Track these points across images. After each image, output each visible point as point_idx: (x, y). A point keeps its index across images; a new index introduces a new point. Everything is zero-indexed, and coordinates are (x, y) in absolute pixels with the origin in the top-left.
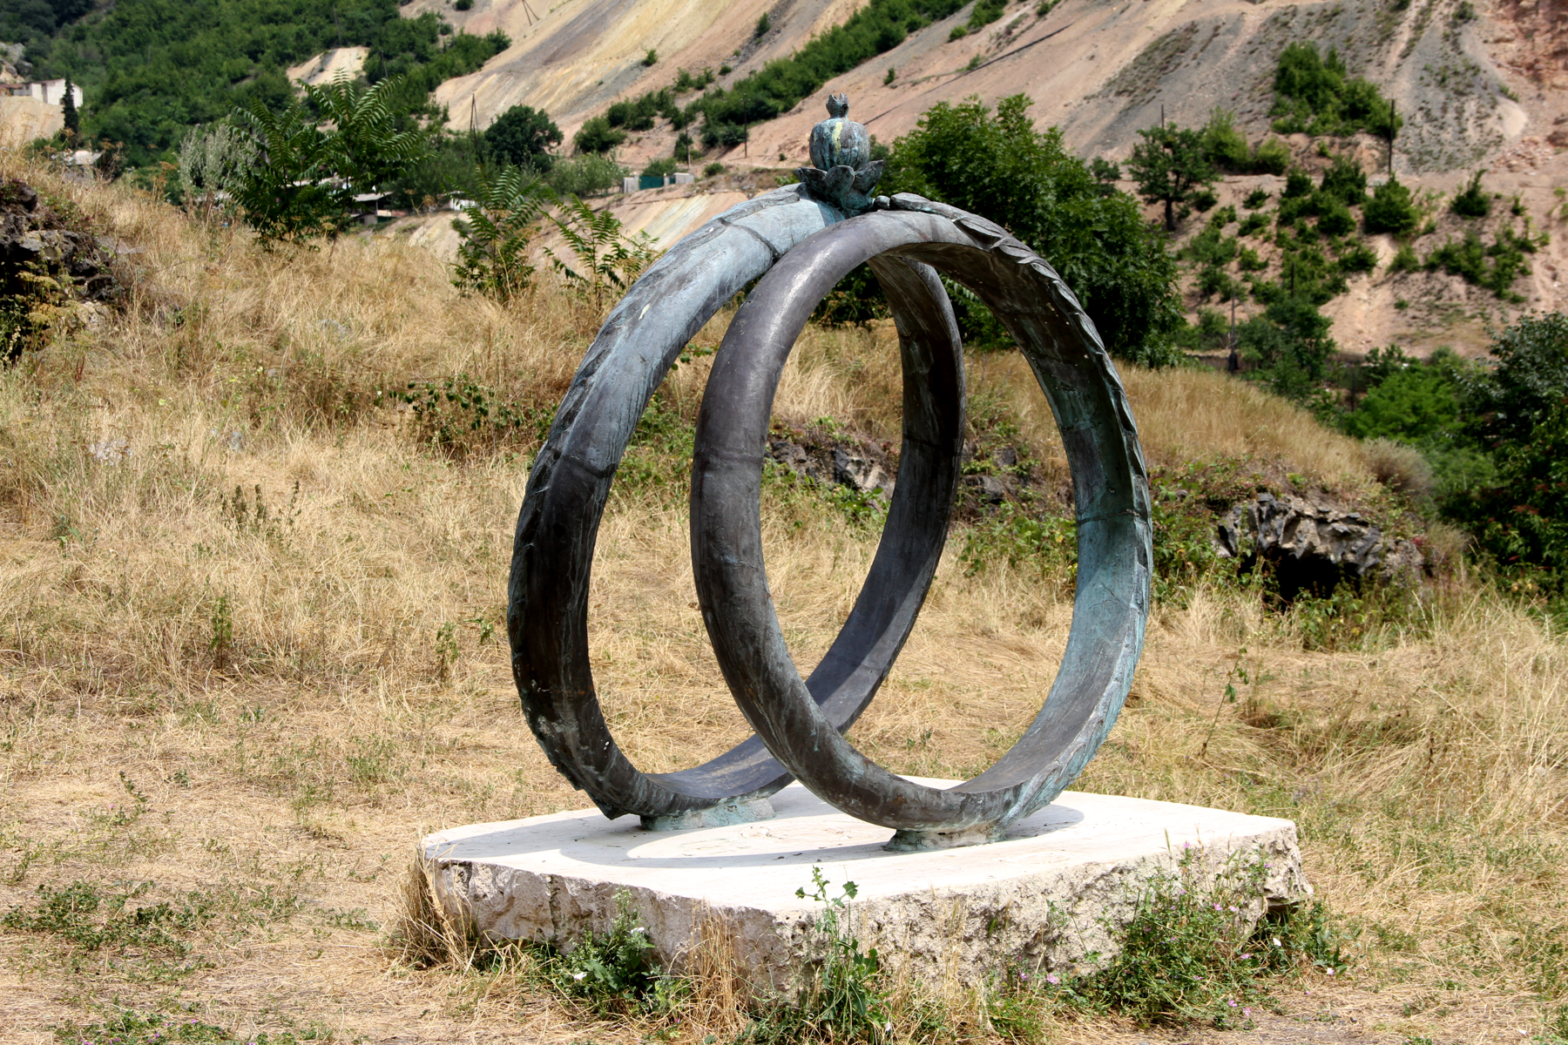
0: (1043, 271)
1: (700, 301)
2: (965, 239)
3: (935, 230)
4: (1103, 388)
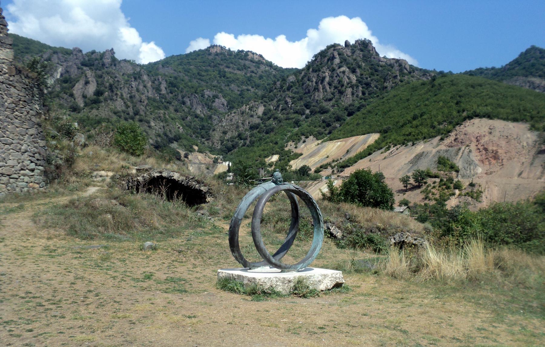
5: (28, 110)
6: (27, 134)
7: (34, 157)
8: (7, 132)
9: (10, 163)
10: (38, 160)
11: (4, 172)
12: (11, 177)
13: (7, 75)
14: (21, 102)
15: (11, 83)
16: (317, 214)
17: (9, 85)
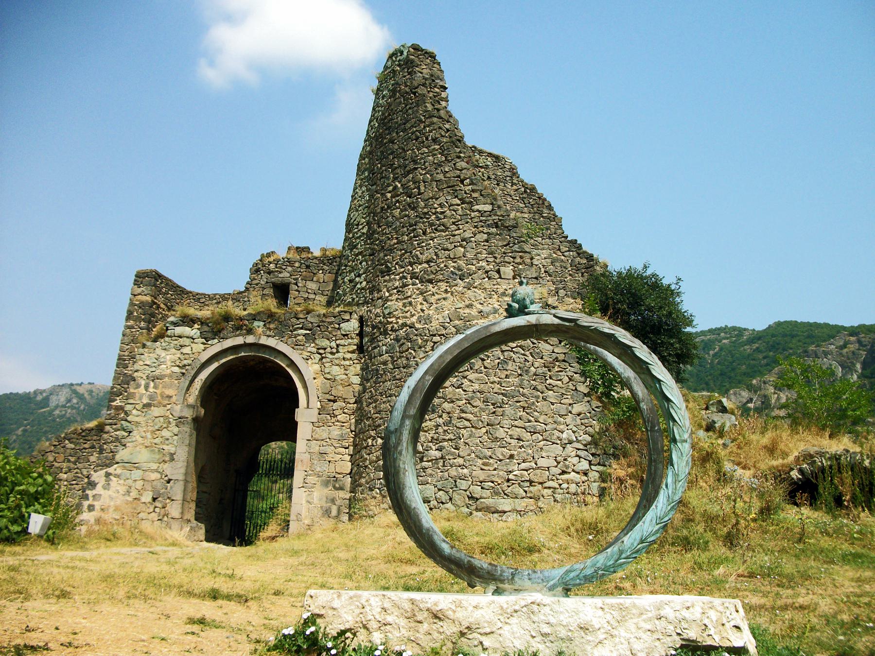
2: (557, 321)
5: (570, 374)
6: (570, 412)
8: (536, 413)
9: (542, 463)
11: (532, 477)
12: (546, 485)
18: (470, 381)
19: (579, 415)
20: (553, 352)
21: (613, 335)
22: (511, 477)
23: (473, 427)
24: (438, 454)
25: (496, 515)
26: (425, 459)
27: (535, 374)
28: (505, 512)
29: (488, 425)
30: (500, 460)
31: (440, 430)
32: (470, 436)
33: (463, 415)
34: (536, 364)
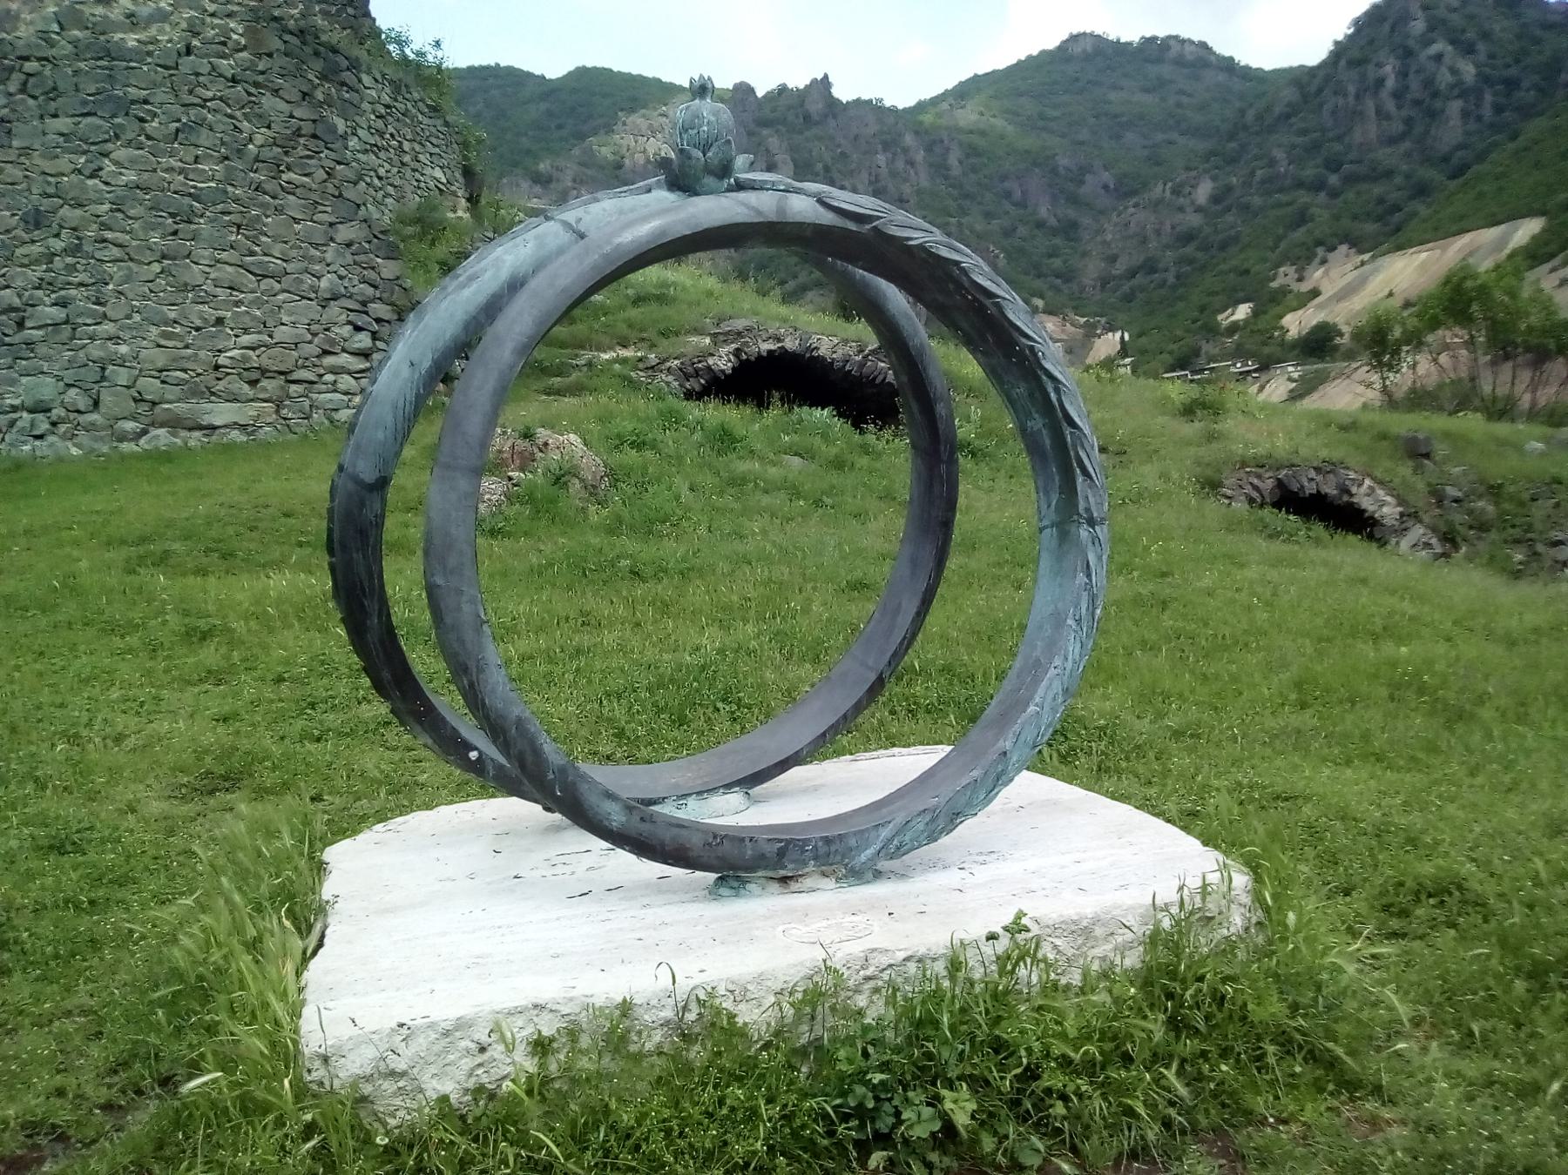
0: (945, 253)
1: (481, 299)
2: (828, 218)
3: (781, 210)
4: (1038, 379)
6: (332, 239)
7: (366, 313)
8: (264, 239)
9: (282, 333)
10: (378, 320)
11: (265, 362)
12: (295, 376)
13: (244, 54)
14: (302, 140)
15: (260, 78)
16: (1058, 421)
17: (256, 85)
18: (116, 163)
19: (349, 245)
20: (292, 116)
21: (957, 263)
22: (222, 360)
23: (131, 260)
24: (58, 314)
25: (197, 434)
26: (29, 324)
27: (257, 160)
28: (215, 428)
29: (164, 257)
30: (198, 329)
31: (58, 263)
32: (128, 279)
33: (109, 235)
34: (259, 139)
